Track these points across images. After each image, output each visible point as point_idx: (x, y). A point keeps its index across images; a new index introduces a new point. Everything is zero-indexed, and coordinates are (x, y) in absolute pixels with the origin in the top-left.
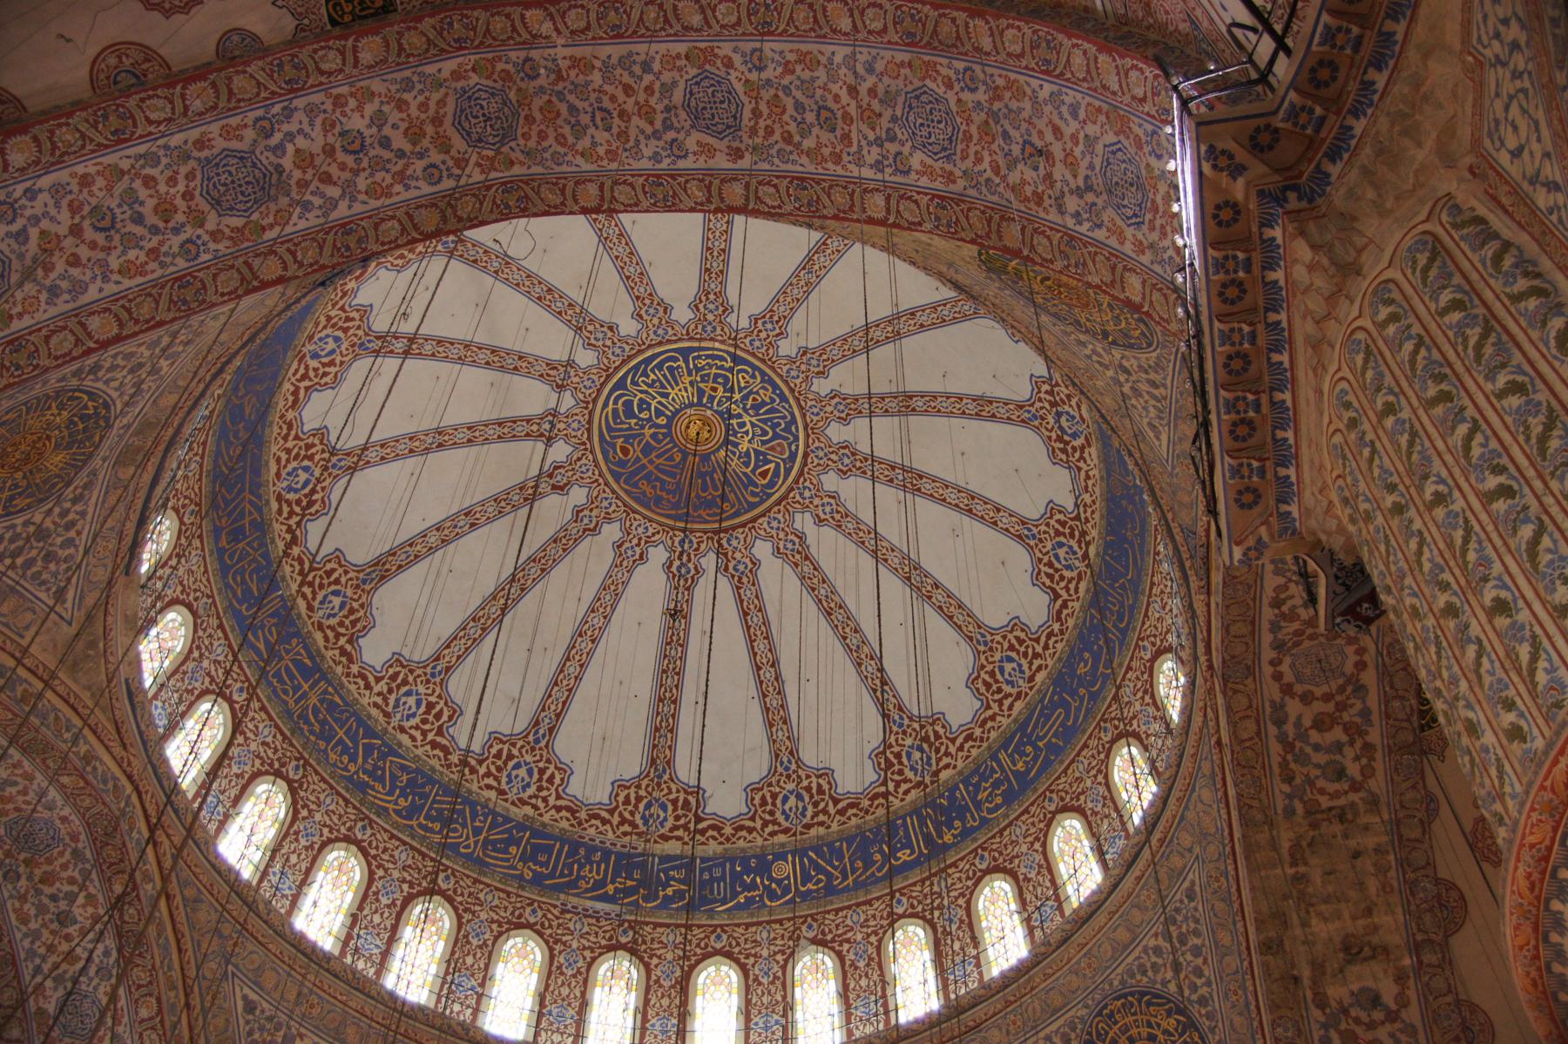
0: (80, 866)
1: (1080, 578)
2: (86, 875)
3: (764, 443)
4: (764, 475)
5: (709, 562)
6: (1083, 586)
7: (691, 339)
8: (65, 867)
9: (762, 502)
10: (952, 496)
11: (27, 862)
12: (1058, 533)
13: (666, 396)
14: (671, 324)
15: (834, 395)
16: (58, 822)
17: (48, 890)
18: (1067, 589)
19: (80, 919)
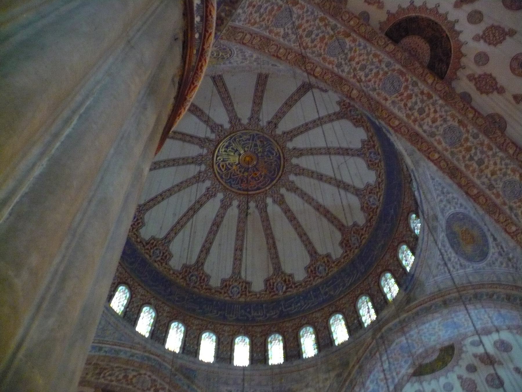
0: (371, 87)
1: (150, 256)
2: (368, 86)
3: (231, 173)
4: (223, 166)
5: (213, 136)
6: (148, 257)
7: (274, 185)
8: (375, 82)
9: (216, 160)
10: (185, 219)
11: (386, 73)
12: (163, 253)
13: (265, 162)
14: (283, 186)
15: (231, 204)
16: (387, 96)
17: (375, 71)
18: (148, 249)
19: (359, 72)
